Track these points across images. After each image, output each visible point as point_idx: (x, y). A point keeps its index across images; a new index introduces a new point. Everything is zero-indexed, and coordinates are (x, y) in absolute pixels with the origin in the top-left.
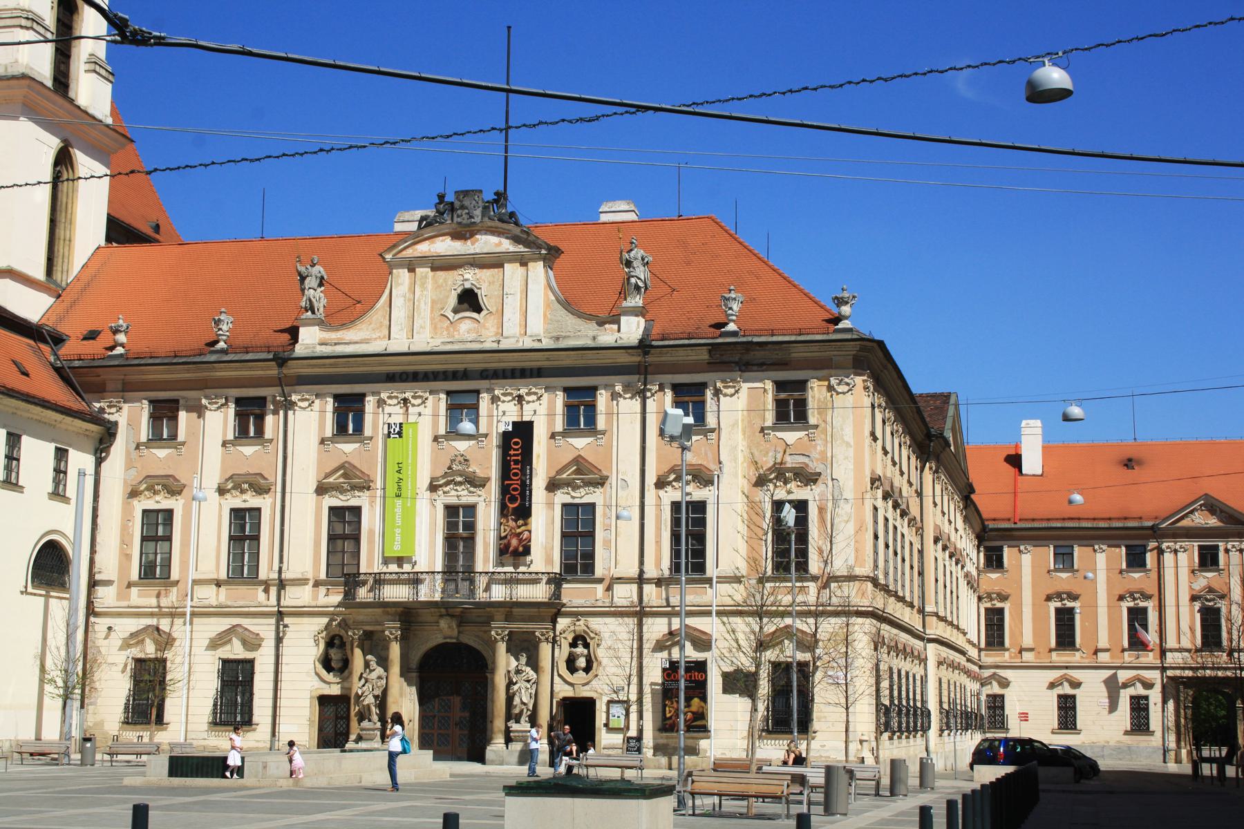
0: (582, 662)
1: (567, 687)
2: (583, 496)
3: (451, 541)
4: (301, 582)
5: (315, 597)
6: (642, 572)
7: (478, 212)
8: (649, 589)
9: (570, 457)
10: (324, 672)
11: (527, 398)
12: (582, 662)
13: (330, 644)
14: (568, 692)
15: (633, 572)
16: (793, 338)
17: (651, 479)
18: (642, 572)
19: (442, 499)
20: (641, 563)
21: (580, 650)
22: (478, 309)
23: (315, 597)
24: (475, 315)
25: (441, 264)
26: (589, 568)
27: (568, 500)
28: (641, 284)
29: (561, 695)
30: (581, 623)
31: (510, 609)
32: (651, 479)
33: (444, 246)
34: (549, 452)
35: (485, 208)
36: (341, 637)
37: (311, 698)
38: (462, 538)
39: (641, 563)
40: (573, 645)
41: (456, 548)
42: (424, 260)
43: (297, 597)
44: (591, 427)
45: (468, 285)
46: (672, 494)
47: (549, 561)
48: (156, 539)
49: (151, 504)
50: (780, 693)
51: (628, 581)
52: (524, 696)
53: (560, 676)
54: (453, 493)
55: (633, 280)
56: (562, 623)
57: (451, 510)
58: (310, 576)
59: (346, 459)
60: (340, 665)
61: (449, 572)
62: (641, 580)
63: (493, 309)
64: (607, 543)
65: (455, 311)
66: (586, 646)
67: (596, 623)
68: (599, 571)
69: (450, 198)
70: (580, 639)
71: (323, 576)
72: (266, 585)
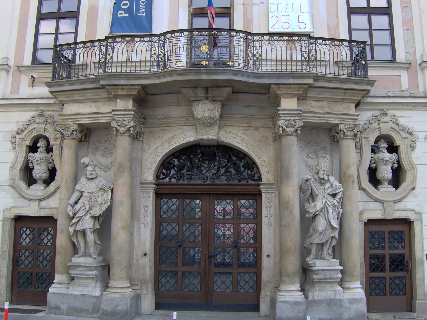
1: (373, 205)
5: (15, 88)
10: (23, 185)
13: (33, 148)
14: (376, 212)
21: (386, 155)
23: (15, 88)
29: (367, 216)
30: (388, 118)
31: (308, 87)
36: (47, 139)
53: (362, 189)
56: (365, 116)
60: (45, 175)
67: (410, 119)
71: (28, 61)
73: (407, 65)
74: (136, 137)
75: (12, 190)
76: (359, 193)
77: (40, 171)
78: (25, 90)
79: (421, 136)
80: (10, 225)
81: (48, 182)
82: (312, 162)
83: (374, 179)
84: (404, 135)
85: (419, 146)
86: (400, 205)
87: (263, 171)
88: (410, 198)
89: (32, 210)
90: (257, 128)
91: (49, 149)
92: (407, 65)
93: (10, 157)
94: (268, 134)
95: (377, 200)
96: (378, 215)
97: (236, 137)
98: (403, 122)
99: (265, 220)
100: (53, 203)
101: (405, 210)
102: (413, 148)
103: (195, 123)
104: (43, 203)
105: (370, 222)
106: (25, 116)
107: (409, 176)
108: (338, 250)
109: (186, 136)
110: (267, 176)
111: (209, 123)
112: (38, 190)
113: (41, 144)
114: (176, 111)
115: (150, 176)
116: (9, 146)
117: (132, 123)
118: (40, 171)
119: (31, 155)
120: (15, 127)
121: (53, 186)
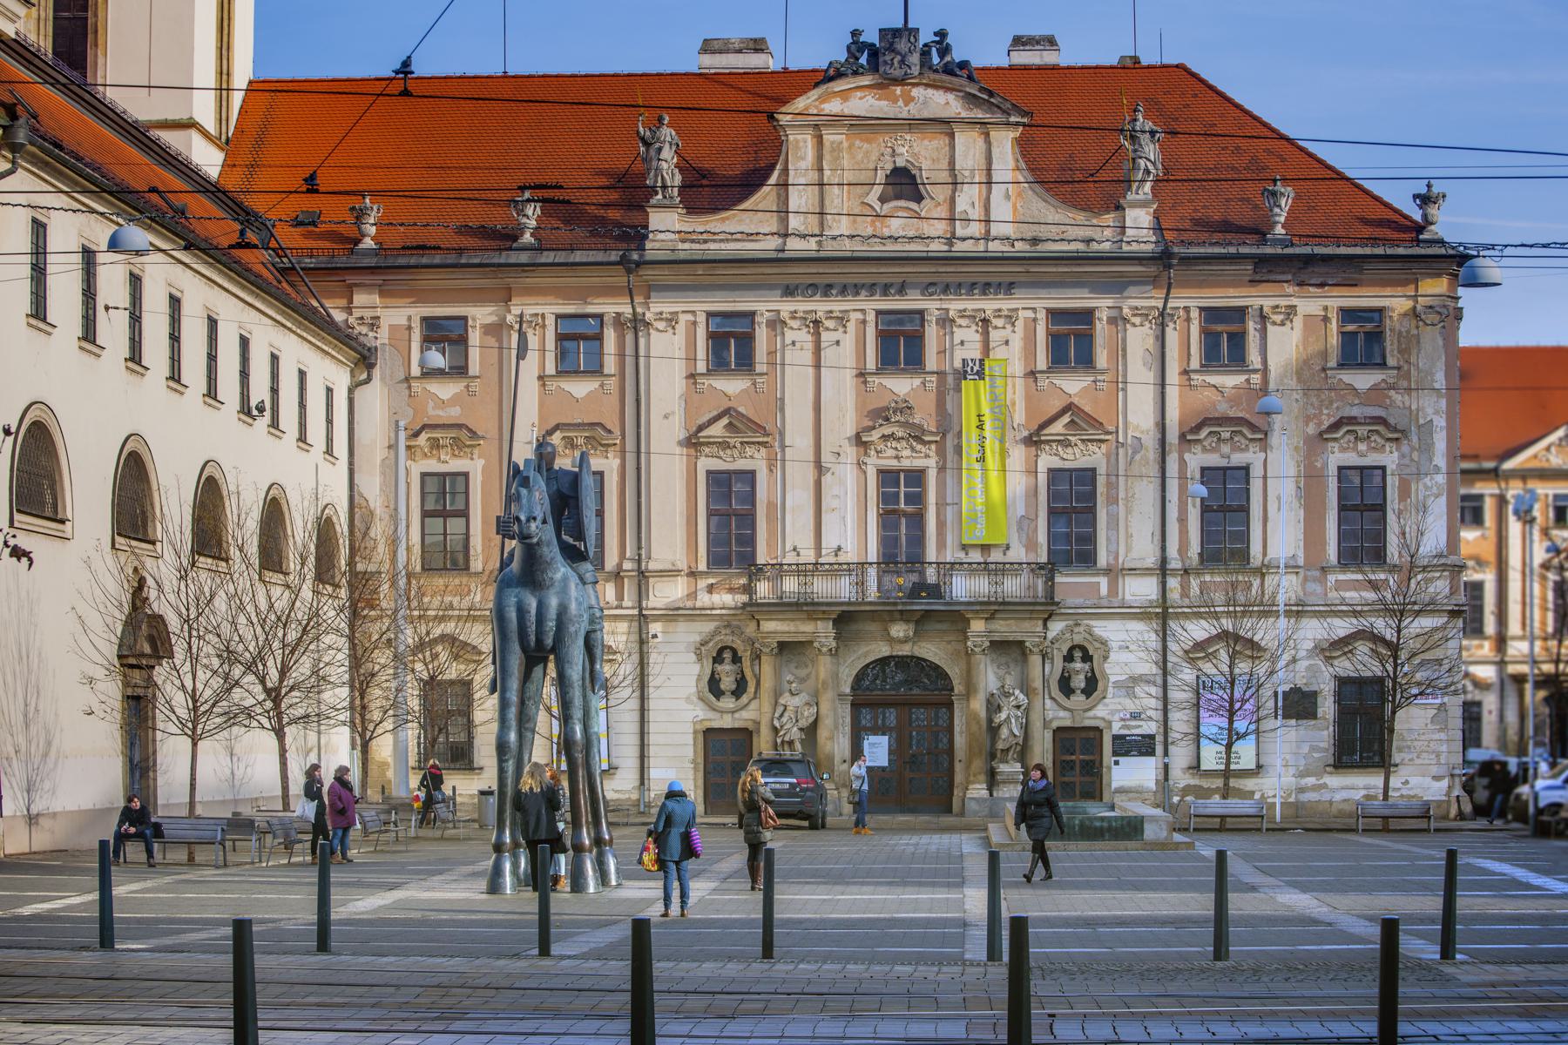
0: (1079, 682)
1: (1062, 714)
2: (1078, 457)
3: (888, 518)
4: (670, 573)
6: (1164, 560)
7: (915, 59)
8: (1173, 583)
9: (1057, 404)
11: (996, 322)
12: (1079, 682)
13: (718, 659)
14: (1063, 719)
15: (1151, 560)
16: (1368, 251)
17: (1173, 436)
18: (1164, 560)
19: (873, 463)
20: (1163, 549)
21: (1078, 665)
22: (919, 198)
23: (693, 595)
24: (913, 205)
25: (862, 125)
26: (1086, 558)
27: (1057, 463)
28: (1151, 167)
29: (1055, 725)
30: (1081, 629)
32: (1173, 436)
33: (864, 102)
34: (1028, 398)
35: (925, 53)
36: (734, 651)
37: (695, 732)
38: (905, 514)
39: (1163, 549)
40: (1069, 658)
41: (897, 527)
42: (836, 120)
43: (665, 593)
44: (1086, 361)
45: (900, 163)
46: (1196, 460)
47: (1031, 545)
48: (444, 514)
49: (432, 466)
50: (1345, 716)
51: (1146, 572)
52: (1010, 731)
54: (890, 452)
55: (1142, 163)
56: (1056, 627)
57: (888, 477)
58: (682, 564)
59: (725, 404)
60: (734, 687)
61: (888, 561)
62: (1163, 570)
63: (941, 199)
64: (1113, 522)
65: (883, 199)
66: (1087, 658)
68: (1103, 559)
69: (871, 36)
70: (1081, 652)
71: (702, 566)
72: (617, 576)
73: (1108, 571)
74: (834, 653)
75: (701, 704)
76: (1048, 702)
77: (727, 683)
78: (704, 599)
79: (1114, 645)
80: (701, 738)
81: (738, 691)
82: (1001, 672)
83: (1066, 686)
84: (1097, 645)
85: (1113, 656)
86: (1091, 714)
87: (955, 682)
88: (1100, 707)
89: (726, 722)
90: (949, 642)
91: (736, 659)
92: (1108, 571)
93: (696, 668)
94: (960, 647)
95: (1065, 709)
96: (1068, 723)
97: (931, 651)
98: (1097, 631)
99: (957, 729)
100: (745, 714)
101: (1096, 718)
102: (1106, 658)
103: (892, 641)
104: (737, 715)
105: (1059, 730)
106: (710, 627)
107: (1100, 685)
108: (1023, 751)
109: (884, 650)
110: (958, 688)
111: (905, 640)
112: (728, 702)
113: (727, 655)
114: (873, 627)
115: (848, 690)
116: (693, 657)
117: (834, 644)
118: (727, 683)
119: (719, 668)
120: (698, 639)
121: (745, 699)
